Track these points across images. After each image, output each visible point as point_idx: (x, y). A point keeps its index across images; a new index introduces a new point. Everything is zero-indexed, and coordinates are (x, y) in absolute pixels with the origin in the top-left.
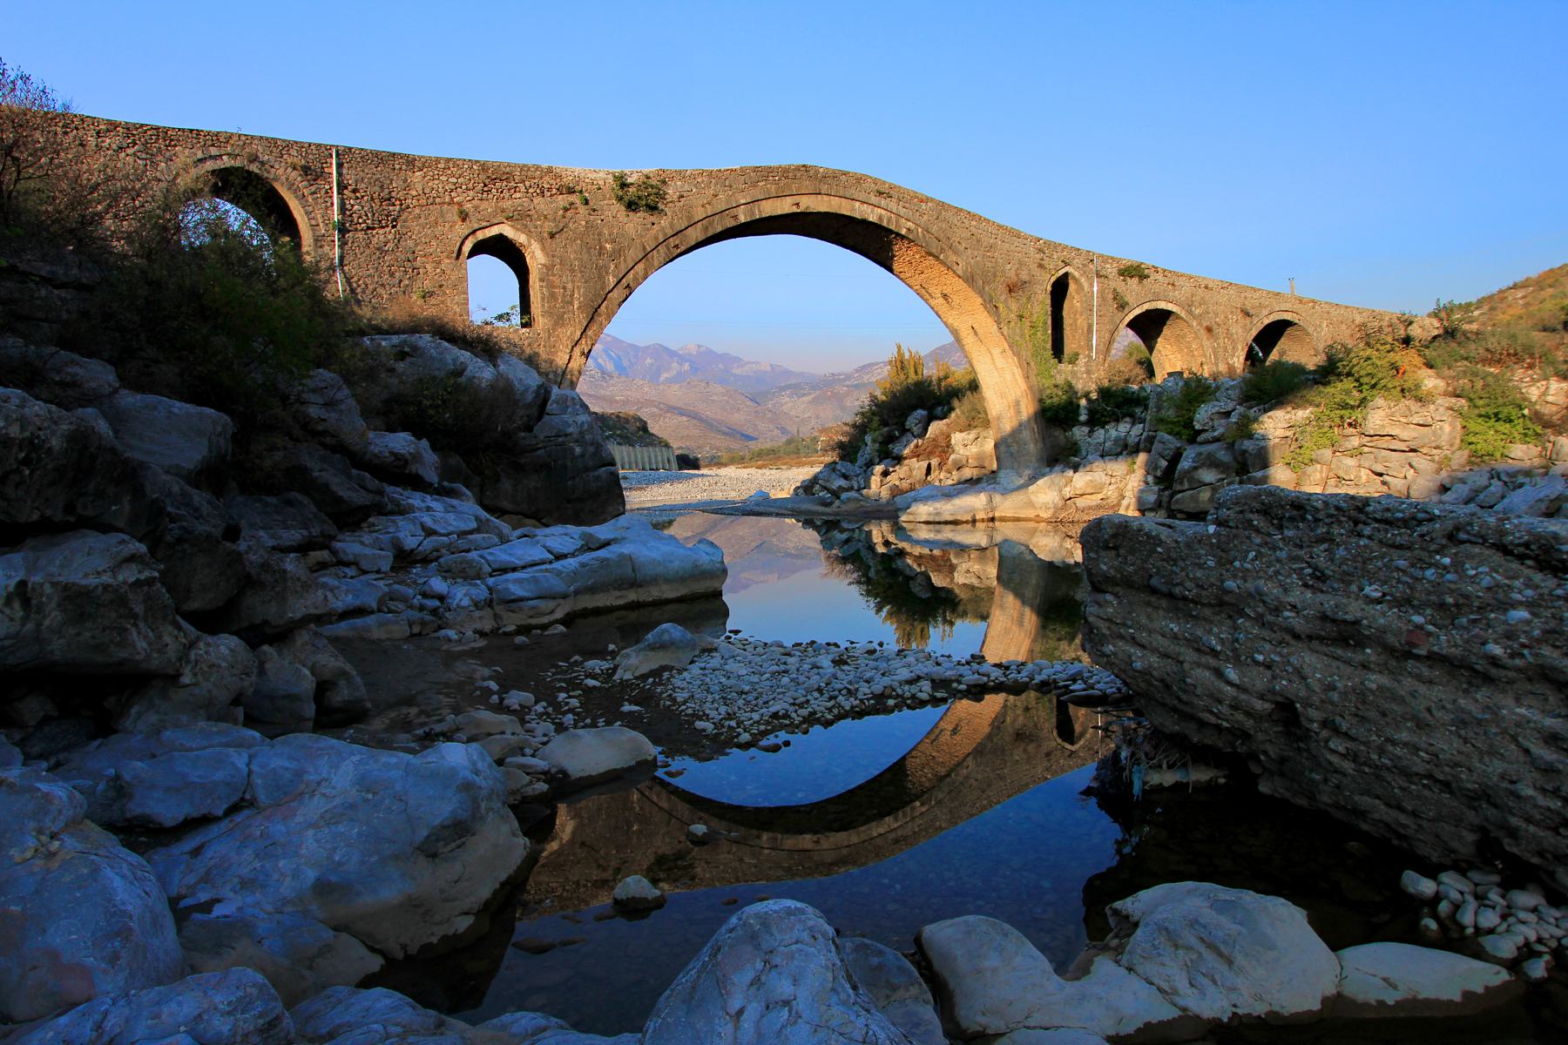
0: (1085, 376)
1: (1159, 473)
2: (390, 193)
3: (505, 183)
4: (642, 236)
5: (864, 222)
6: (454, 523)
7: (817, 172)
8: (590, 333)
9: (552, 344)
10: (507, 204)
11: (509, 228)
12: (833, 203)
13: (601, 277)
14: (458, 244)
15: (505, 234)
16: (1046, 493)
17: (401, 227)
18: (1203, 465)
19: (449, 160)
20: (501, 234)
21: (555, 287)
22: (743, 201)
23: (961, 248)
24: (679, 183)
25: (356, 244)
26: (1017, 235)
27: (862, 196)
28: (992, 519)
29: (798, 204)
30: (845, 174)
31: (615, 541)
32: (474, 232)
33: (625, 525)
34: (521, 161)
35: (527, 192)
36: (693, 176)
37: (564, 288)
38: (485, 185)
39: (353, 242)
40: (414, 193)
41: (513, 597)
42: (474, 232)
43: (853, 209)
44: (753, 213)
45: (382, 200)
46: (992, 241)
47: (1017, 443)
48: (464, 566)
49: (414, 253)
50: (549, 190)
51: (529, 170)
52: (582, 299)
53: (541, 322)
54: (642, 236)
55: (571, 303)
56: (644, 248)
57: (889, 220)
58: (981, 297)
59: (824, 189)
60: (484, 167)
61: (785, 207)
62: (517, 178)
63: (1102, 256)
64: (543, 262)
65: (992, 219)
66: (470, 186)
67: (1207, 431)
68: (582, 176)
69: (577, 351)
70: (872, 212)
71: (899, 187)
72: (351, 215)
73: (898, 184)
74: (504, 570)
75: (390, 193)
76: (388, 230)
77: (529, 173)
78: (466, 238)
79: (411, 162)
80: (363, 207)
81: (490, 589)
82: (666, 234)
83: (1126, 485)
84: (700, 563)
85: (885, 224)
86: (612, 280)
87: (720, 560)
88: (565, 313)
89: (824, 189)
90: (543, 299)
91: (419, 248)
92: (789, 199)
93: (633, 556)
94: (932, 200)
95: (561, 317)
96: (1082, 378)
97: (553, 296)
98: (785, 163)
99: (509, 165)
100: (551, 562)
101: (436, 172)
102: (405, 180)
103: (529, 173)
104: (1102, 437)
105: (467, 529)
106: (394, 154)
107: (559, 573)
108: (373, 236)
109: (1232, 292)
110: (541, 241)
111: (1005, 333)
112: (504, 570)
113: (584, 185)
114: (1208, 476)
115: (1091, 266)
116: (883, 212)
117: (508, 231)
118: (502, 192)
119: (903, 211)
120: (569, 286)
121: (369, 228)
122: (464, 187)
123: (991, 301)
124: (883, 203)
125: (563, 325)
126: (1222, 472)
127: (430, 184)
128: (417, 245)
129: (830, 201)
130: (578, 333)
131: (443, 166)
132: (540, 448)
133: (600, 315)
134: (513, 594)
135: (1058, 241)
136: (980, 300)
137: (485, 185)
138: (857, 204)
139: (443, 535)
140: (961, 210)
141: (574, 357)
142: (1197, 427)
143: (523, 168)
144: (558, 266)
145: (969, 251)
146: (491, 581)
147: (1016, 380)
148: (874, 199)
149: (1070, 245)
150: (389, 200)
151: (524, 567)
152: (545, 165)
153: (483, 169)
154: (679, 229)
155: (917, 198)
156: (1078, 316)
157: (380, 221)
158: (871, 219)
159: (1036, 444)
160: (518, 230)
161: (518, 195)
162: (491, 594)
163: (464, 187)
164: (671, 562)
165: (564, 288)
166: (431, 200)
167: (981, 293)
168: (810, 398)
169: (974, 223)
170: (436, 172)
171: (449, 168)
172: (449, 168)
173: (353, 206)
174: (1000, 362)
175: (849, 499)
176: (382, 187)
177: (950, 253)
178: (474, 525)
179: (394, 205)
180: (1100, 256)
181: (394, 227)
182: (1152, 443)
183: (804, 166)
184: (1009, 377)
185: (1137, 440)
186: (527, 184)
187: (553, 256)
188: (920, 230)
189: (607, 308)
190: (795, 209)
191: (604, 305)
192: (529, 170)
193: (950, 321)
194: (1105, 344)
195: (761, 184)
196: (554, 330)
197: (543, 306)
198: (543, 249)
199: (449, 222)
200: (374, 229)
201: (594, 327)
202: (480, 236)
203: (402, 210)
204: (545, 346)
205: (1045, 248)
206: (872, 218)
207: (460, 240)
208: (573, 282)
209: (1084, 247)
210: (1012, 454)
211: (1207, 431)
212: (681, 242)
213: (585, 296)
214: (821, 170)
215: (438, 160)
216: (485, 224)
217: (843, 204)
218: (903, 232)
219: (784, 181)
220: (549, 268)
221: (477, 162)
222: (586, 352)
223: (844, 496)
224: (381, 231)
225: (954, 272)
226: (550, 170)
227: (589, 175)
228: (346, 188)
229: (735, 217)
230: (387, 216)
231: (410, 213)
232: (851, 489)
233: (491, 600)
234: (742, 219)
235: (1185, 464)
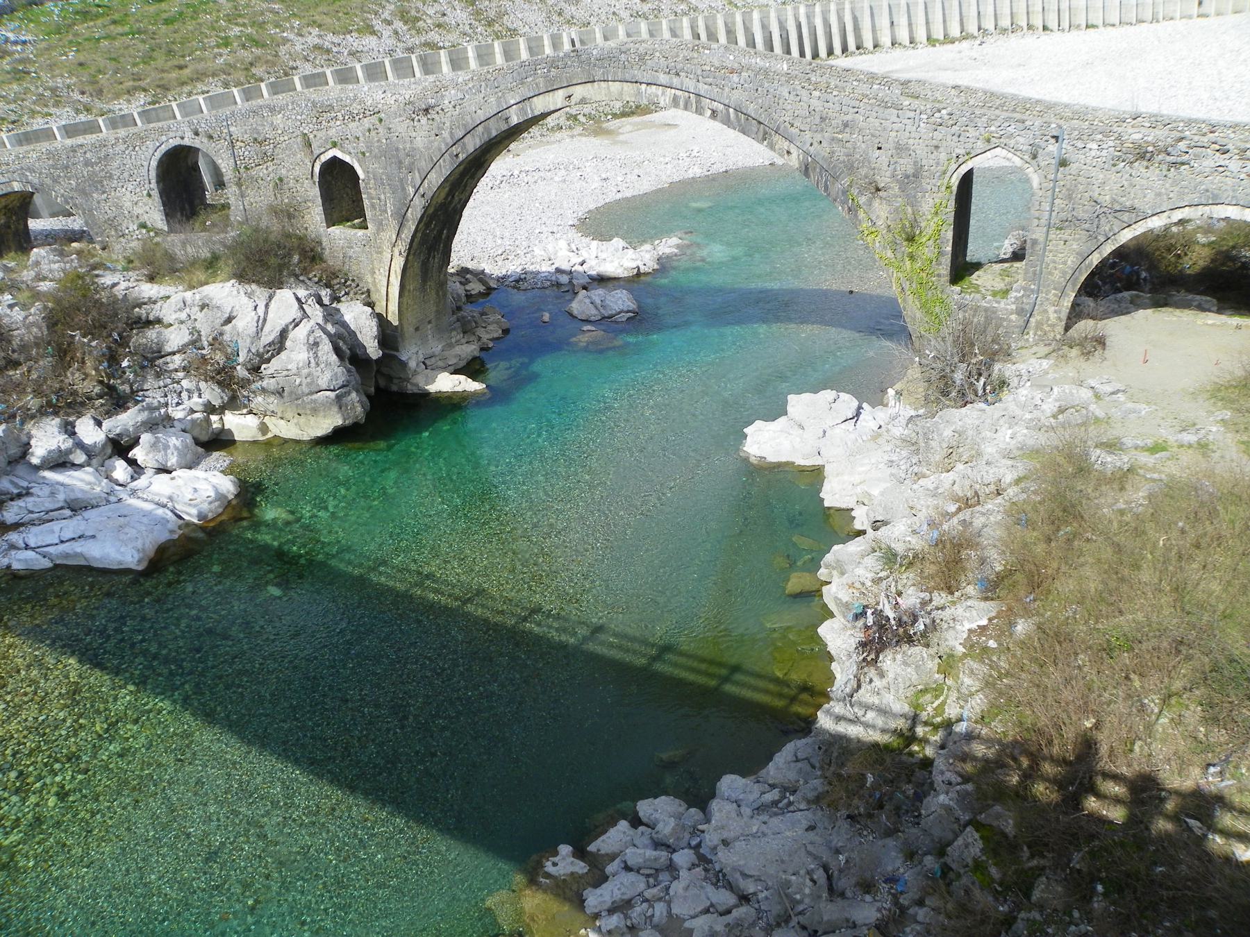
4: (429, 149)
12: (612, 89)
13: (404, 189)
22: (512, 102)
23: (794, 131)
24: (453, 92)
27: (647, 77)
37: (379, 199)
43: (639, 93)
44: (526, 113)
54: (429, 149)
55: (386, 211)
56: (432, 160)
59: (599, 74)
70: (663, 93)
78: (315, 161)
82: (447, 144)
86: (411, 191)
89: (599, 74)
92: (561, 92)
116: (679, 93)
119: (703, 89)
120: (382, 197)
124: (676, 81)
129: (608, 88)
130: (394, 237)
138: (644, 86)
145: (808, 135)
148: (663, 78)
165: (379, 199)
189: (412, 214)
195: (529, 79)
208: (385, 194)
213: (394, 205)
214: (595, 52)
216: (323, 150)
219: (554, 72)
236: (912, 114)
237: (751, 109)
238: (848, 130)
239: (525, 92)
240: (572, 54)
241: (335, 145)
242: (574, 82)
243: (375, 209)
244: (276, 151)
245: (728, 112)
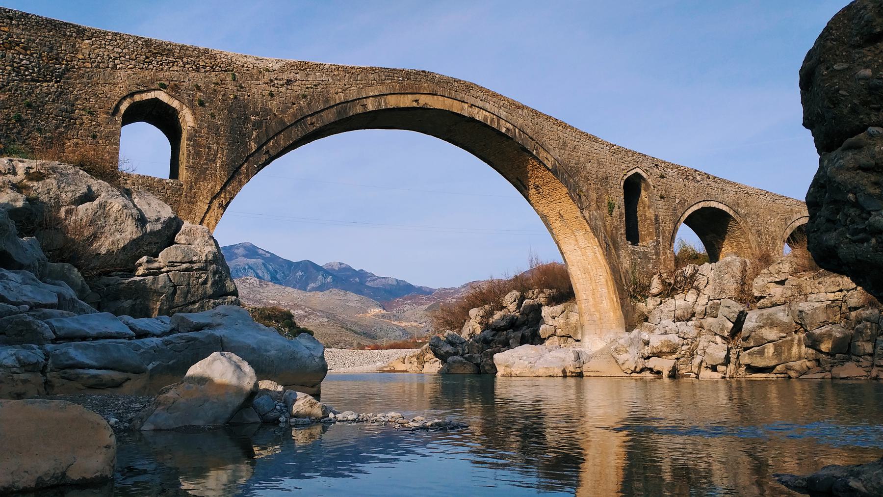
0: (654, 257)
1: (726, 334)
2: (58, 54)
3: (165, 58)
5: (472, 120)
6: (30, 294)
7: (434, 77)
8: (229, 188)
9: (193, 195)
10: (165, 75)
11: (165, 94)
14: (115, 103)
15: (160, 98)
16: (627, 351)
17: (65, 83)
18: (765, 325)
19: (116, 34)
20: (156, 98)
21: (201, 147)
22: (371, 94)
25: (19, 92)
26: (595, 140)
27: (472, 101)
28: (580, 375)
29: (417, 101)
30: (457, 81)
31: (209, 326)
32: (132, 95)
33: (222, 312)
34: (181, 42)
35: (184, 67)
36: (330, 70)
37: (209, 148)
38: (147, 58)
39: (16, 90)
40: (81, 57)
41: (70, 362)
42: (132, 95)
43: (463, 109)
44: (380, 104)
45: (50, 58)
46: (576, 143)
47: (599, 312)
48: (20, 328)
49: (73, 105)
50: (204, 67)
51: (187, 49)
52: (224, 159)
53: (184, 174)
55: (214, 161)
57: (492, 120)
58: (567, 187)
60: (148, 43)
61: (406, 101)
62: (176, 55)
63: (665, 162)
64: (192, 124)
65: (576, 127)
66: (133, 56)
67: (764, 297)
68: (234, 59)
69: (216, 203)
71: (501, 95)
72: (18, 68)
73: (499, 93)
74: (70, 338)
75: (58, 54)
76: (51, 84)
77: (188, 52)
78: (124, 98)
79: (81, 32)
80: (31, 62)
81: (47, 355)
83: (697, 346)
84: (299, 356)
85: (489, 123)
87: (320, 355)
88: (207, 169)
90: (189, 156)
91: (79, 102)
93: (225, 340)
94: (527, 108)
95: (204, 172)
96: (652, 259)
97: (198, 154)
98: (408, 68)
99: (170, 44)
100: (130, 338)
101: (103, 42)
102: (74, 46)
103: (188, 52)
104: (673, 306)
105: (44, 302)
106: (67, 23)
107: (137, 348)
108: (37, 87)
109: (769, 198)
110: (192, 107)
111: (587, 217)
112: (70, 338)
113: (235, 66)
114: (771, 334)
115: (656, 169)
117: (163, 96)
118: (161, 65)
119: (503, 114)
120: (215, 147)
121: (33, 80)
122: (127, 57)
123: (575, 191)
125: (205, 179)
126: (782, 331)
127: (96, 51)
128: (77, 99)
130: (218, 188)
131: (110, 37)
132: (164, 272)
133: (240, 174)
134: (72, 359)
135: (629, 148)
136: (565, 190)
137: (147, 58)
139: (13, 304)
140: (550, 117)
141: (213, 208)
142: (756, 294)
143: (182, 47)
144: (205, 130)
146: (49, 347)
147: (596, 257)
149: (639, 151)
150: (56, 59)
151: (96, 338)
152: (202, 47)
153: (146, 45)
154: (316, 110)
155: (514, 104)
156: (646, 209)
157: (45, 76)
158: (477, 118)
159: (615, 313)
160: (172, 96)
161: (176, 68)
162: (46, 360)
163: (127, 57)
164: (267, 351)
165: (209, 148)
166: (96, 64)
167: (566, 183)
168: (426, 307)
169: (561, 128)
170: (103, 42)
171: (116, 41)
172: (116, 41)
173: (22, 60)
174: (582, 242)
175: (454, 362)
176: (51, 49)
177: (541, 150)
178: (55, 300)
179: (60, 64)
180: (662, 162)
181: (57, 82)
182: (717, 309)
183: (423, 71)
184: (590, 255)
185: (704, 308)
186: (185, 60)
187: (202, 121)
188: (517, 130)
189: (246, 168)
190: (415, 105)
191: (245, 166)
192: (187, 49)
193: (541, 209)
194: (670, 232)
195: (388, 82)
196: (196, 184)
197: (188, 162)
198: (194, 114)
199: (109, 84)
200: (38, 81)
201: (235, 183)
202: (137, 98)
203: (67, 70)
204: (186, 196)
205: (617, 151)
206: (479, 116)
207: (119, 99)
209: (650, 153)
210: (594, 321)
211: (764, 297)
212: (317, 120)
213: (228, 157)
215: (106, 33)
216: (142, 88)
217: (455, 104)
218: (504, 130)
220: (196, 132)
221: (141, 38)
222: (224, 203)
223: (450, 359)
224: (45, 84)
225: (545, 166)
226: (206, 51)
227: (240, 59)
228: (18, 45)
229: (364, 106)
230: (51, 72)
231: (74, 72)
232: (456, 354)
233: (45, 366)
234: (370, 108)
235: (749, 324)
236: (602, 146)
237: (528, 131)
238: (576, 150)
239: (382, 89)
240: (422, 73)
241: (163, 87)
242: (422, 92)
243: (201, 158)
244: (68, 74)
245: (515, 129)
